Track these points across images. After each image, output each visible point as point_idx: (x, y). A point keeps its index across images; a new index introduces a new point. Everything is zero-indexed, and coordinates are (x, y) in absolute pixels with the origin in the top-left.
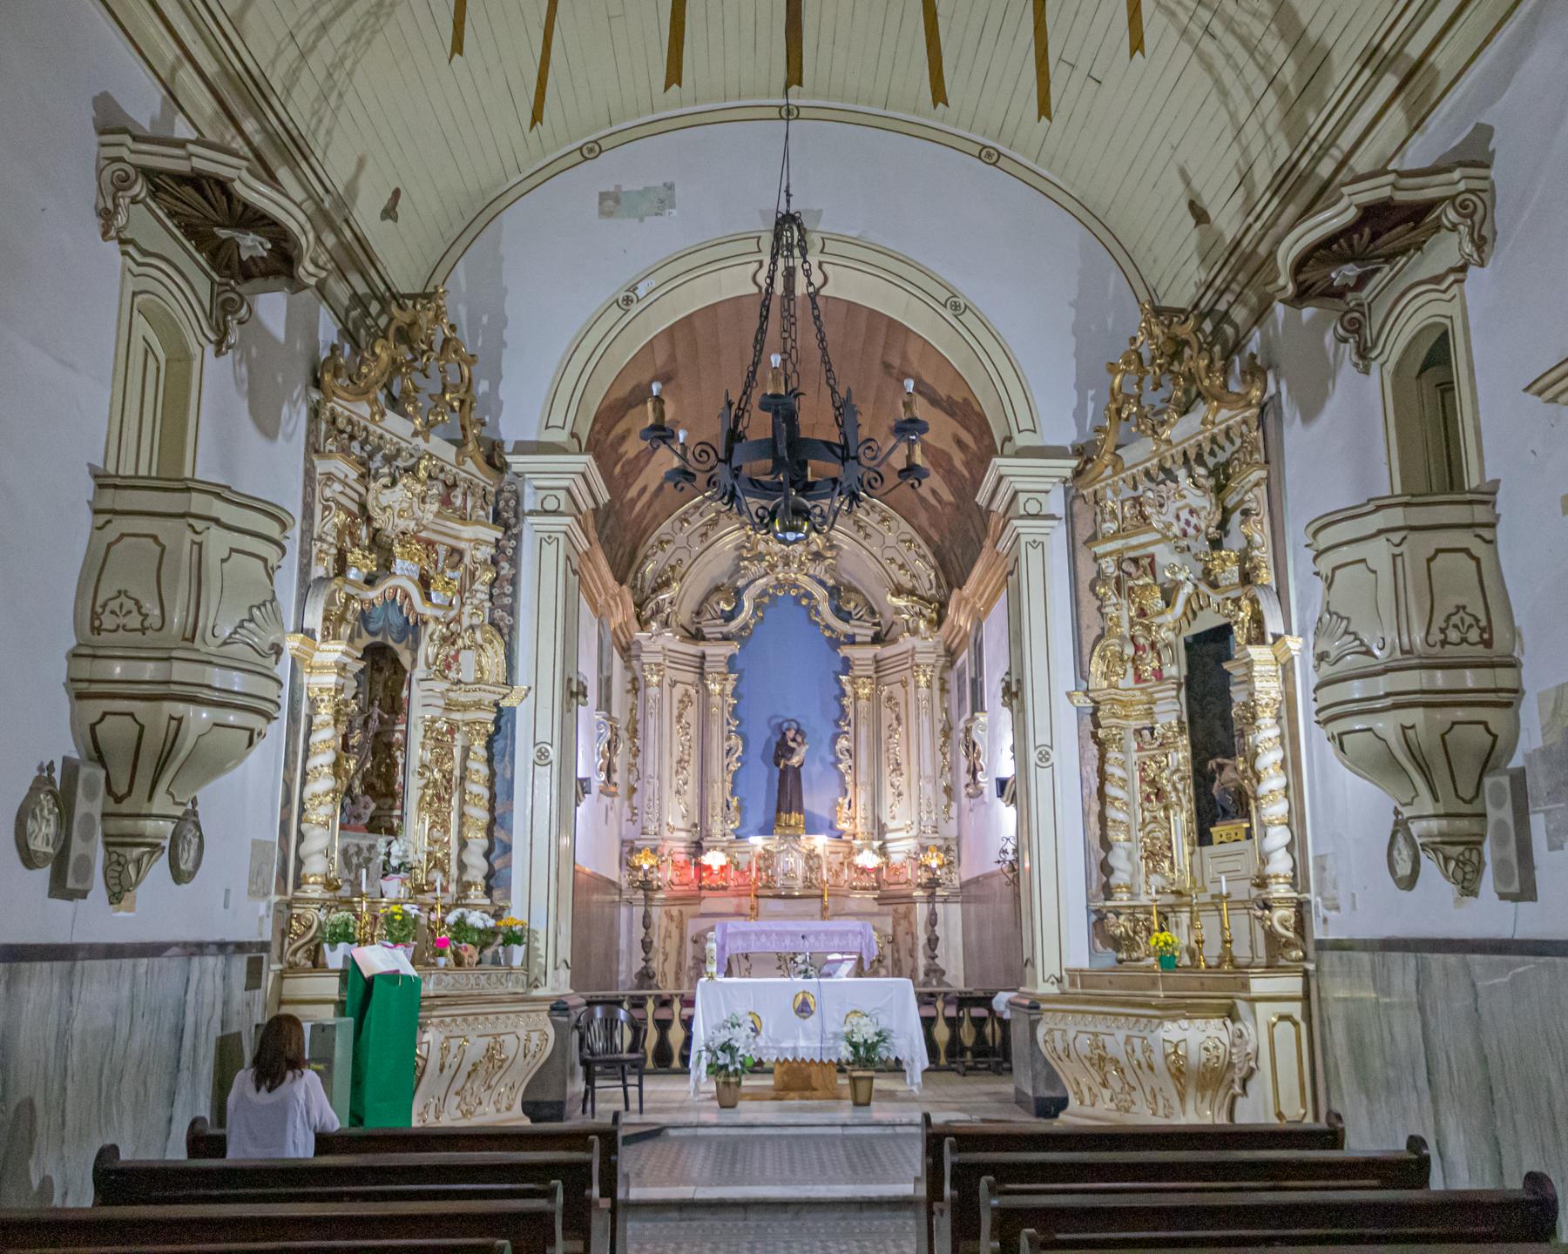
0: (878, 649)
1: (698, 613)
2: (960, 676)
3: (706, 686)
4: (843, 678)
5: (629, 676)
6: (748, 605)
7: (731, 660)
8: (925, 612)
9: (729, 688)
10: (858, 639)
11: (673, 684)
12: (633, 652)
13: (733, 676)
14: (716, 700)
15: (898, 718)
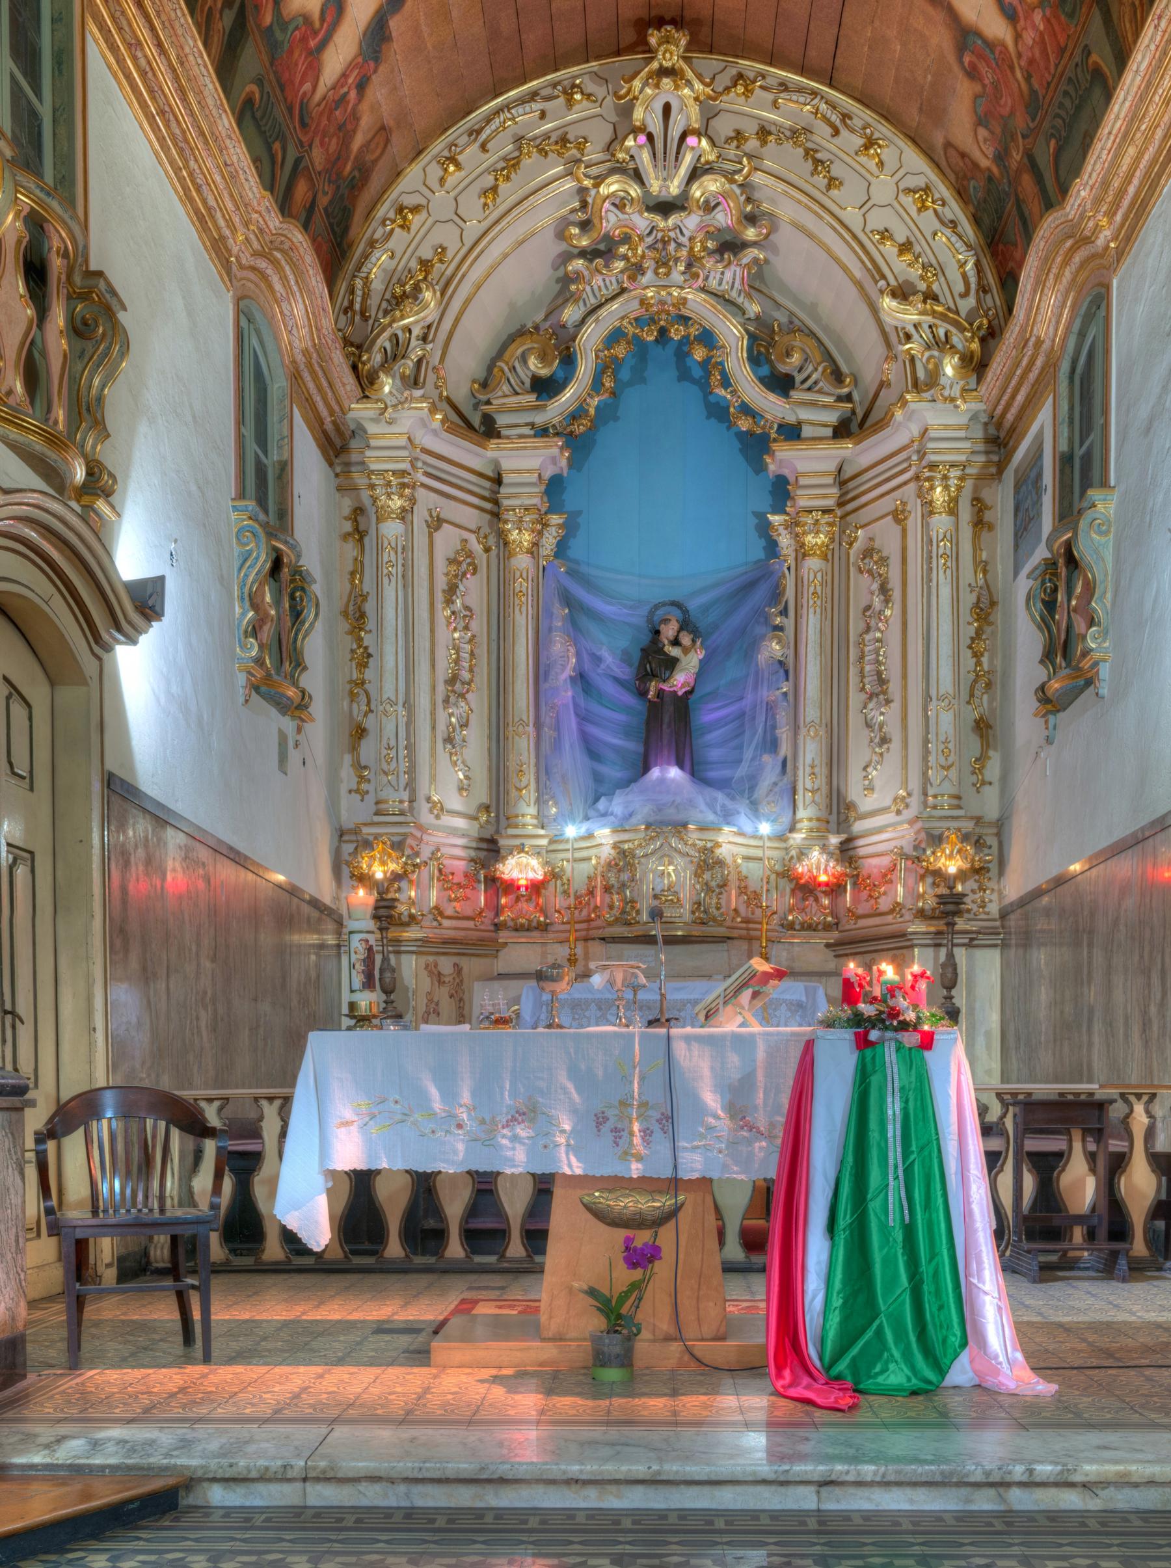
0: (846, 448)
1: (484, 385)
2: (1028, 483)
3: (502, 536)
4: (776, 519)
5: (347, 504)
6: (585, 369)
7: (554, 487)
8: (957, 339)
9: (549, 541)
10: (807, 431)
11: (436, 523)
12: (354, 457)
13: (555, 519)
14: (522, 562)
15: (884, 590)
